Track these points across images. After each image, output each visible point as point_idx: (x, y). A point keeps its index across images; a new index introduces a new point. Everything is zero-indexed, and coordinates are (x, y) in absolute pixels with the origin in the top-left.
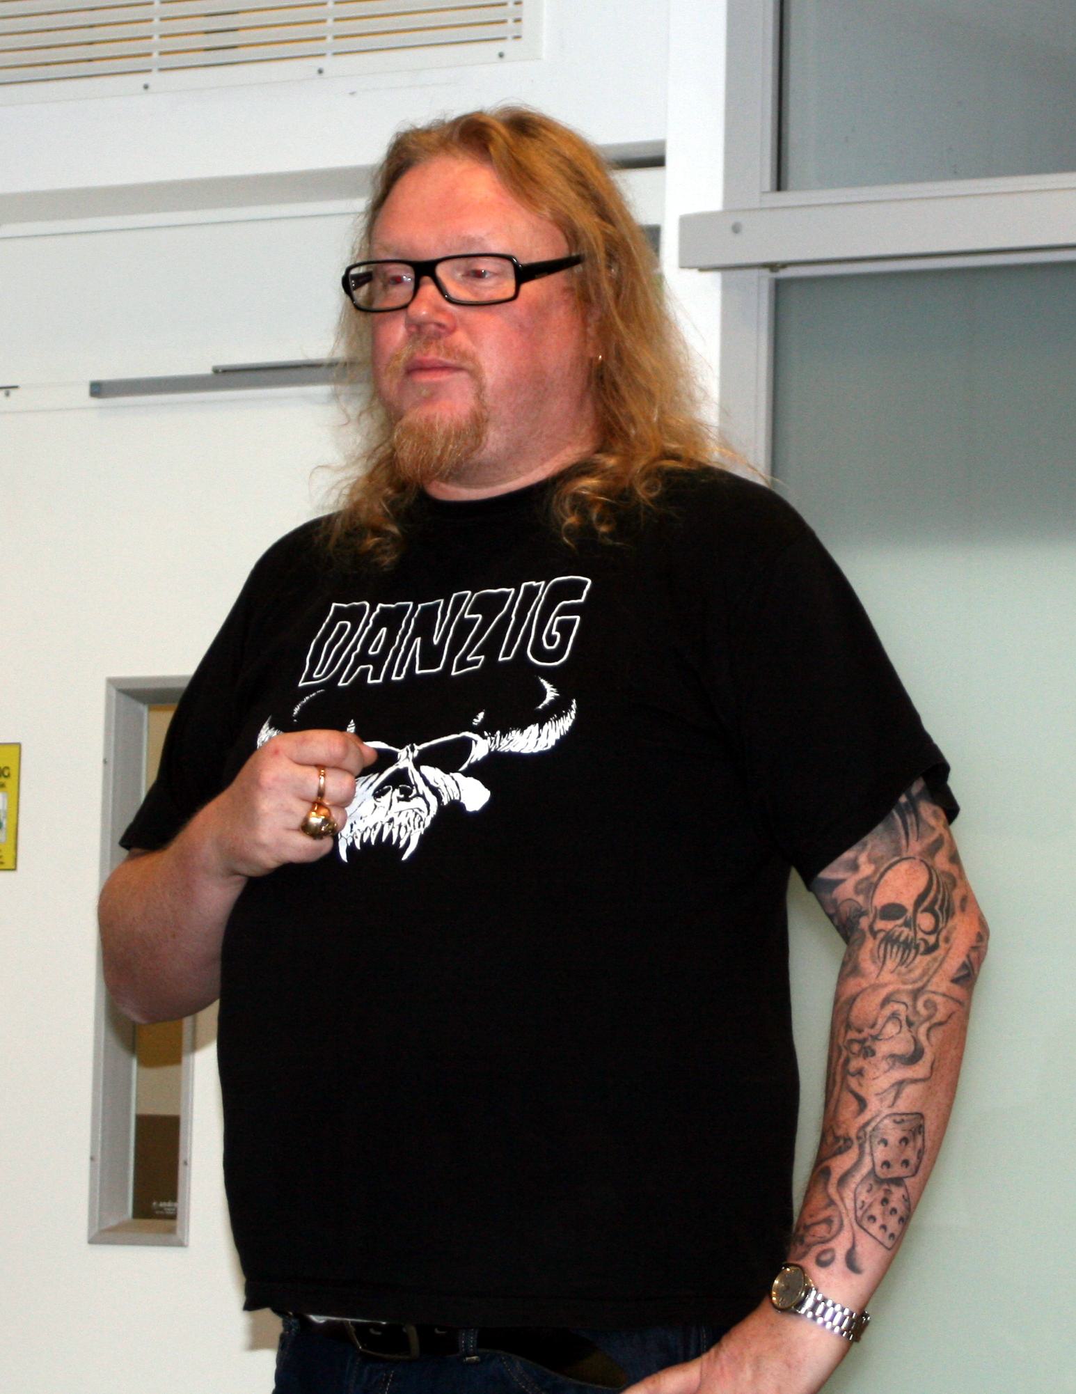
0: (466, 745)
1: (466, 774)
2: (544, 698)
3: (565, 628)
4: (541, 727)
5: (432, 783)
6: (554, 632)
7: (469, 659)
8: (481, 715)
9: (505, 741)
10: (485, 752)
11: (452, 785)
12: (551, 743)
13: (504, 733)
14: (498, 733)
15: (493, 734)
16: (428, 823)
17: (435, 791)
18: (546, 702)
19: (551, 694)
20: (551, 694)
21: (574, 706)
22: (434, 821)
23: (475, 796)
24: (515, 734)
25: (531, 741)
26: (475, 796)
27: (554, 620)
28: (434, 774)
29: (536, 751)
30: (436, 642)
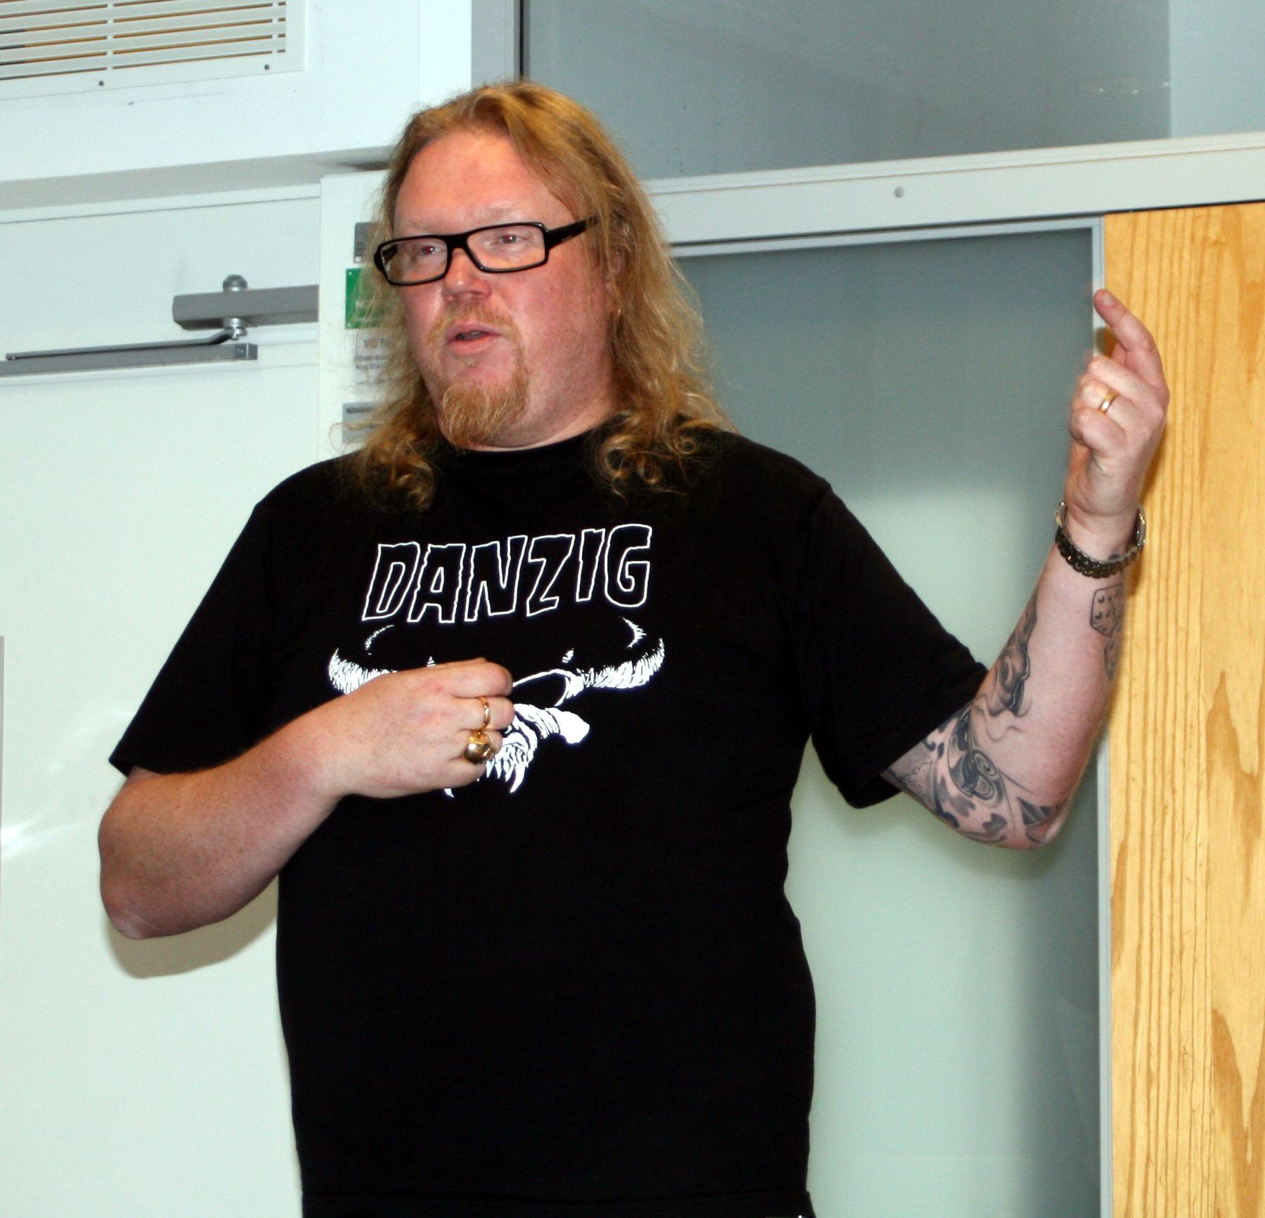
0: (559, 683)
1: (563, 708)
3: (637, 572)
4: (634, 664)
5: (526, 718)
7: (542, 600)
8: (570, 654)
9: (599, 678)
10: (581, 689)
11: (549, 719)
12: (646, 679)
13: (598, 670)
14: (592, 670)
15: (586, 672)
16: (531, 757)
17: (532, 726)
18: (635, 641)
19: (638, 634)
20: (638, 634)
21: (661, 645)
22: (535, 753)
23: (574, 729)
24: (609, 671)
26: (574, 729)
27: (624, 565)
28: (528, 711)
29: (631, 686)
30: (504, 586)
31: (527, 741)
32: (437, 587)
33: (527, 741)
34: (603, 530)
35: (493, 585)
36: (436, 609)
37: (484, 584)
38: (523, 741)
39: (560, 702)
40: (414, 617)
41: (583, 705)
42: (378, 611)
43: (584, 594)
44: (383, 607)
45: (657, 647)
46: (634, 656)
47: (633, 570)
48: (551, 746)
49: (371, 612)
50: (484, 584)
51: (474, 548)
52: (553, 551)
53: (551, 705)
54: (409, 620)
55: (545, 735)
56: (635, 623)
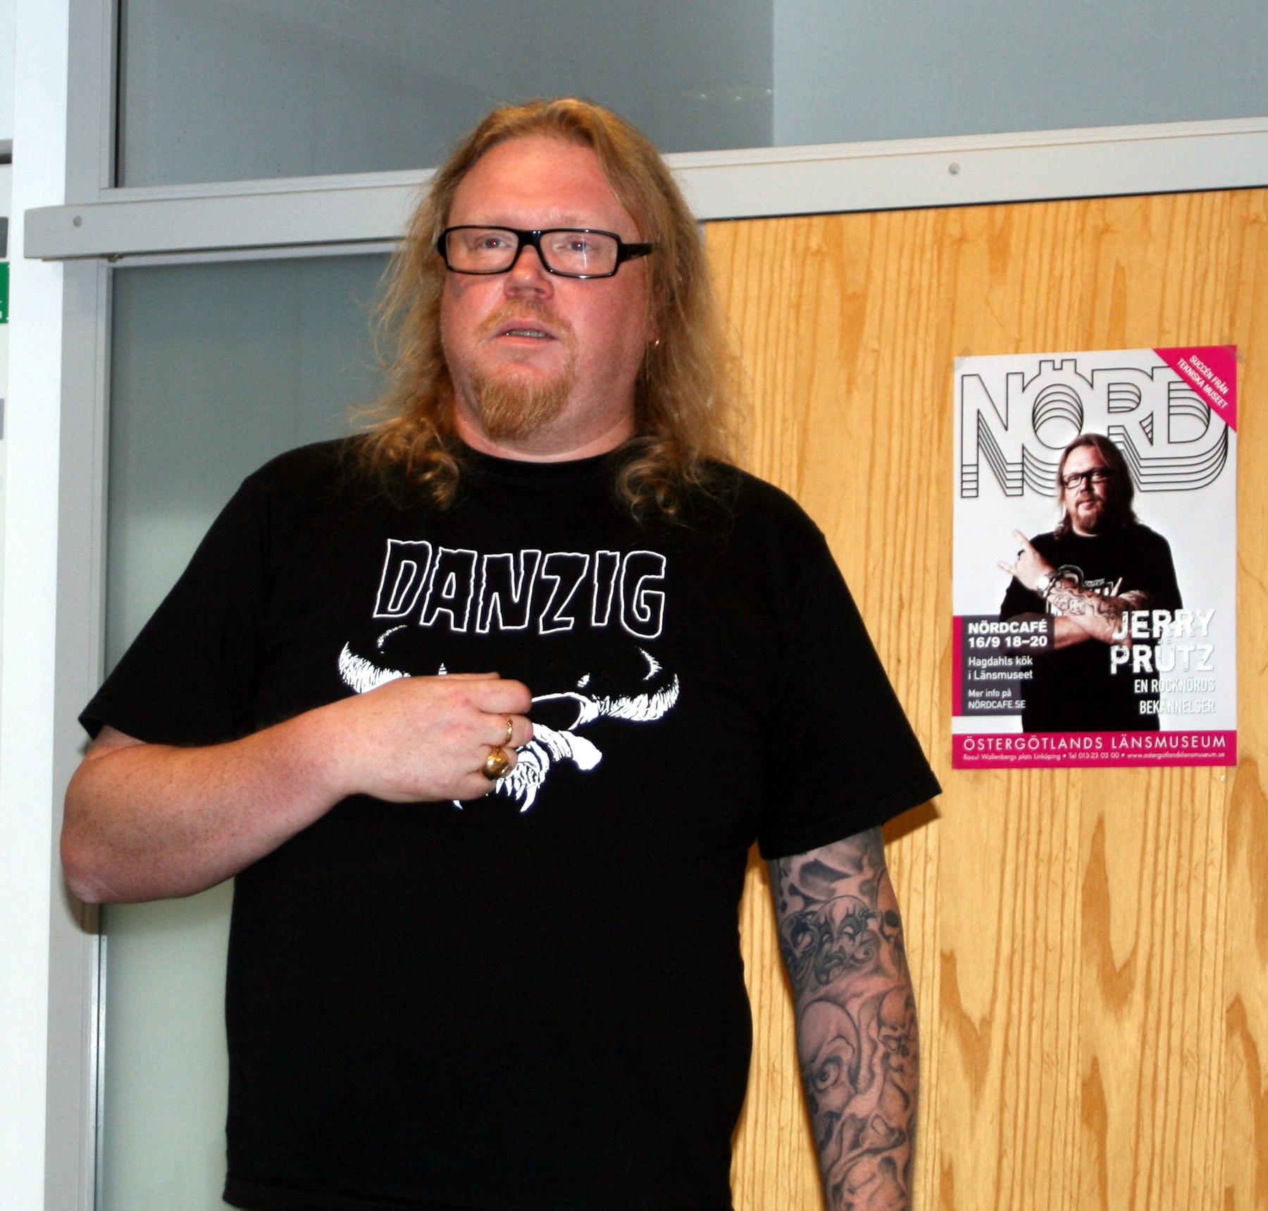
0: (574, 708)
1: (577, 733)
2: (647, 668)
4: (650, 698)
6: (643, 605)
8: (586, 679)
9: (615, 707)
10: (596, 715)
11: (562, 742)
12: (660, 714)
15: (602, 699)
16: (543, 779)
17: (544, 747)
18: (651, 674)
19: (654, 667)
20: (654, 667)
22: (547, 775)
23: (587, 756)
24: (624, 701)
25: (642, 709)
26: (587, 756)
27: (640, 594)
28: (541, 731)
31: (539, 761)
32: (449, 593)
33: (539, 761)
34: (618, 554)
35: (505, 597)
36: (447, 616)
37: (496, 595)
38: (535, 761)
39: (574, 726)
40: (427, 619)
41: (597, 732)
42: (389, 609)
43: (600, 618)
44: (394, 606)
45: (672, 683)
46: (652, 688)
47: (649, 599)
48: (563, 770)
49: (383, 609)
50: (496, 595)
51: (486, 557)
52: (569, 570)
53: (565, 729)
54: (422, 623)
55: (557, 758)
56: (651, 654)
